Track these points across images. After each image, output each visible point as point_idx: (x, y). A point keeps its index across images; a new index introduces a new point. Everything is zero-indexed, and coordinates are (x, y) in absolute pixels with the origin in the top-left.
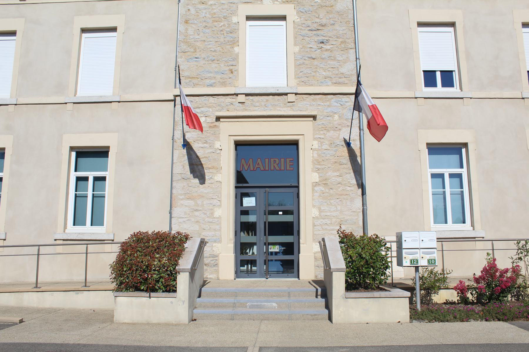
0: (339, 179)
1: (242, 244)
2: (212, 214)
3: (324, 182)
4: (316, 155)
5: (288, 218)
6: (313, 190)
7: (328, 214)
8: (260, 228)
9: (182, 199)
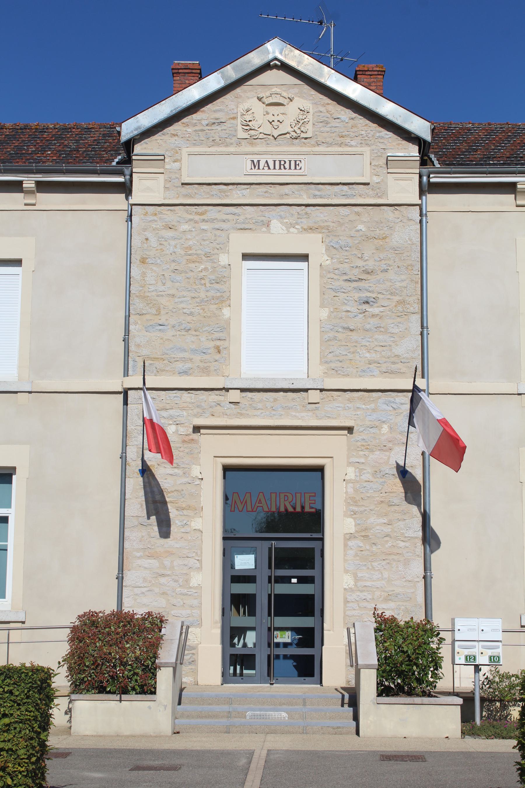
0: (387, 529)
1: (232, 628)
2: (187, 581)
3: (363, 533)
4: (350, 490)
5: (306, 589)
6: (346, 545)
7: (368, 584)
8: (262, 603)
9: (140, 558)
